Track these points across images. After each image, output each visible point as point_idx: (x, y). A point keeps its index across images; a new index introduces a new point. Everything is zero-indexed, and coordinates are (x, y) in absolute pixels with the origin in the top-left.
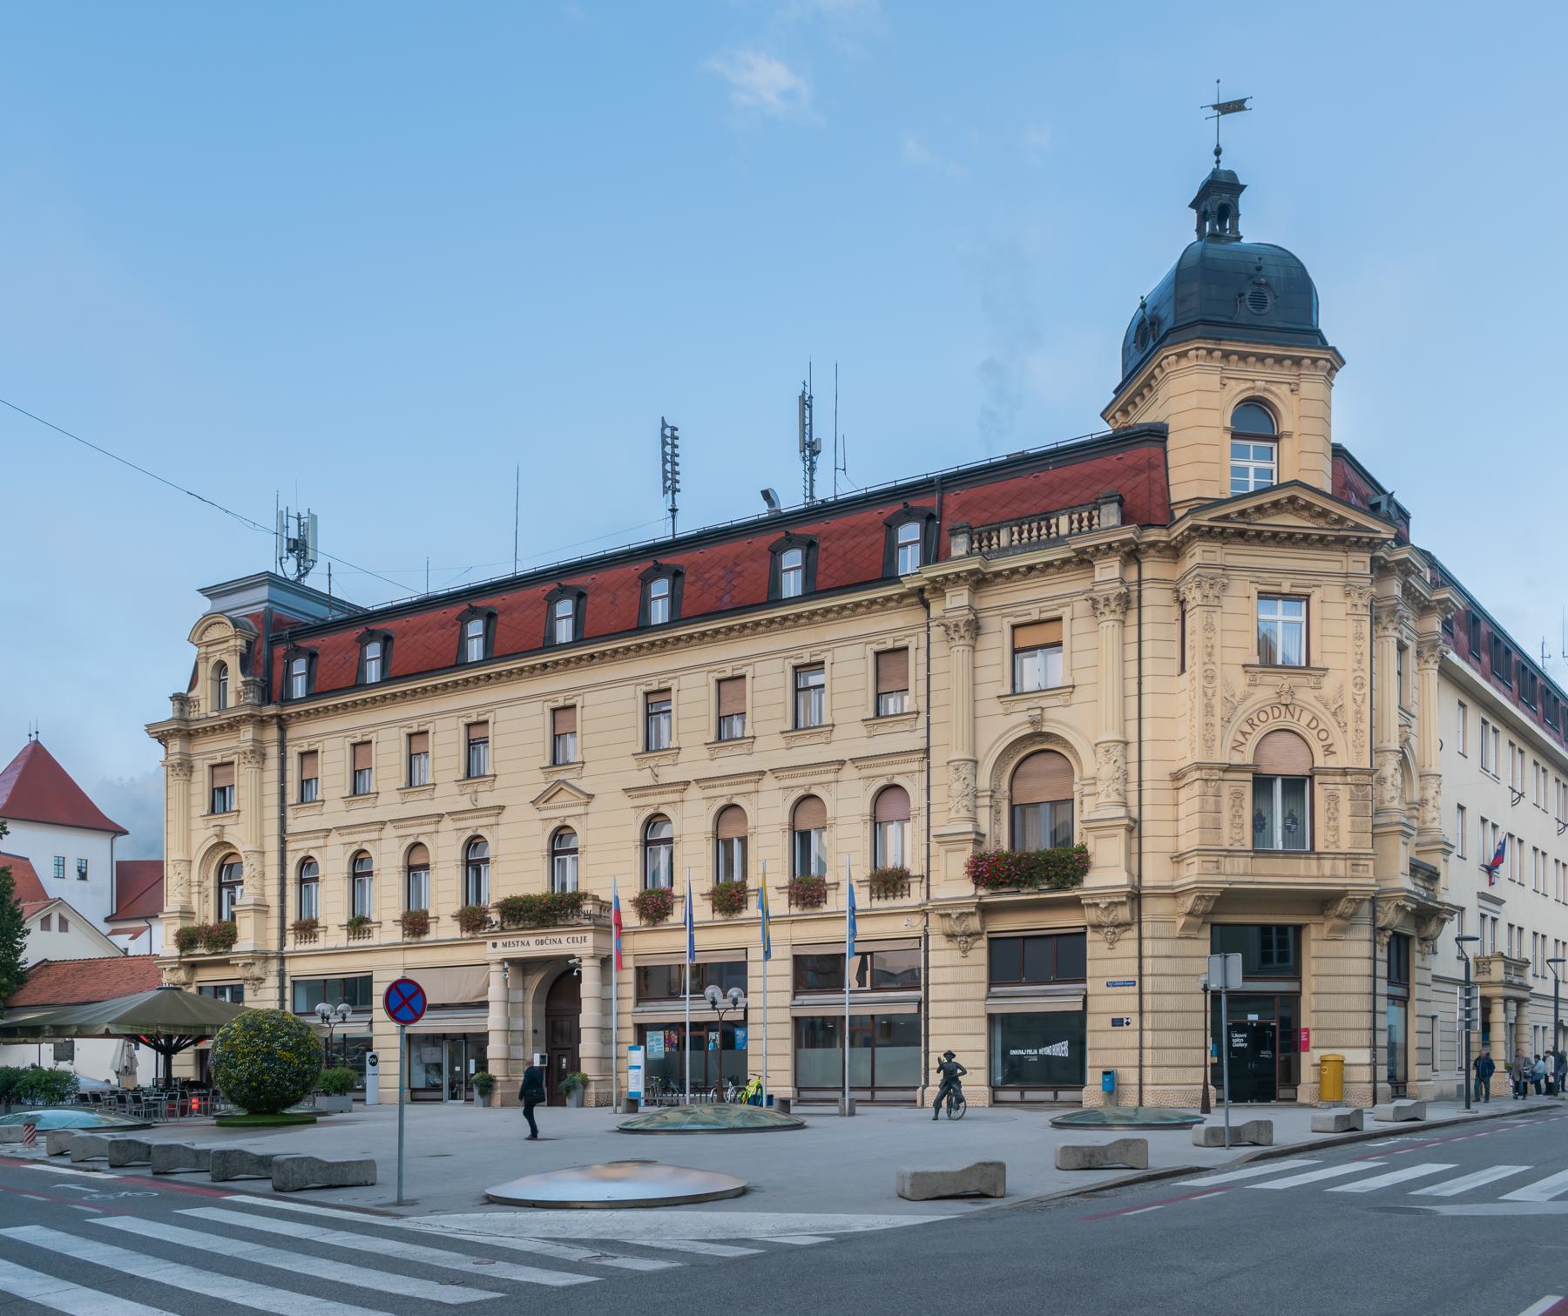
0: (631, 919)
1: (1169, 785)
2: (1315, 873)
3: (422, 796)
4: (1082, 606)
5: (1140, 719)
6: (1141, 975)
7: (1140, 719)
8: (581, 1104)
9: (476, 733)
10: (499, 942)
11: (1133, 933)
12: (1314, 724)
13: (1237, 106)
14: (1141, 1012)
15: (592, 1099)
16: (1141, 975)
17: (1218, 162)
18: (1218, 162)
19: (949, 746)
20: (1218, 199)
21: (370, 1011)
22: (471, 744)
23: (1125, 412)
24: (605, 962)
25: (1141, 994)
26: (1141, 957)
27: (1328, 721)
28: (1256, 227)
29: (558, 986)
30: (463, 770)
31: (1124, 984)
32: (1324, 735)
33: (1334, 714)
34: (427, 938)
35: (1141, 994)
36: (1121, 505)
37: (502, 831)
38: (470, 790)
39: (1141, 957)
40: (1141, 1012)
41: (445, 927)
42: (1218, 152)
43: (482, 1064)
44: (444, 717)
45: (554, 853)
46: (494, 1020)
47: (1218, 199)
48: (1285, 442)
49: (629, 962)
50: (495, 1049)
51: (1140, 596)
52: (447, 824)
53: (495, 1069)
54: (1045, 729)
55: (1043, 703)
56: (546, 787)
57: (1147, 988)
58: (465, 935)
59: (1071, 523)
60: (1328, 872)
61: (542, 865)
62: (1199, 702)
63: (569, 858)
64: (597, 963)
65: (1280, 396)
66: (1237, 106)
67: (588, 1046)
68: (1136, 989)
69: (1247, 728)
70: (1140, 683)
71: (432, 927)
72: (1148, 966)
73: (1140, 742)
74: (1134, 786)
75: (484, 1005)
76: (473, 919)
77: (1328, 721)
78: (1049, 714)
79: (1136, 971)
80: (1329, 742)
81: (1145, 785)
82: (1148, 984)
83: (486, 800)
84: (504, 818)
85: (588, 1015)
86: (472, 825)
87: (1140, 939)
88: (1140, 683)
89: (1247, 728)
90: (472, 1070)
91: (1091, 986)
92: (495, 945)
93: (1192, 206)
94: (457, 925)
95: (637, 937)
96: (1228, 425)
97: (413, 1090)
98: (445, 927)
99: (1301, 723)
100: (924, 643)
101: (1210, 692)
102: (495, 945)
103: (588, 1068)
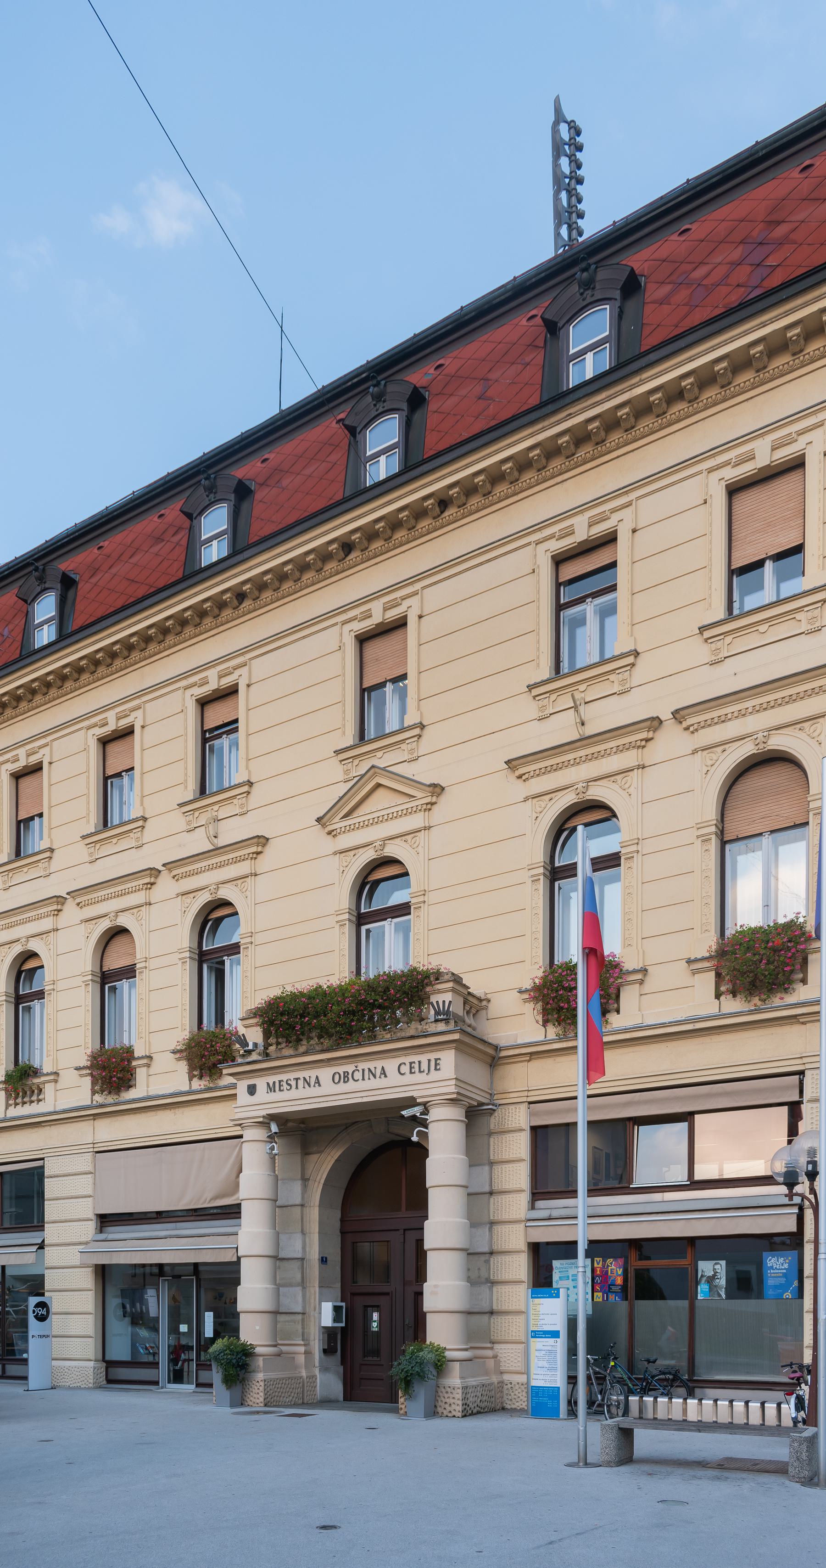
0: (517, 1023)
3: (124, 844)
8: (432, 1412)
9: (217, 715)
10: (261, 1083)
15: (454, 1402)
21: (41, 1227)
22: (208, 738)
24: (476, 1116)
29: (373, 1173)
30: (192, 785)
34: (132, 1094)
37: (262, 887)
38: (203, 819)
41: (163, 1073)
43: (228, 1323)
44: (158, 700)
45: (361, 919)
46: (251, 1236)
49: (520, 1118)
50: (252, 1293)
52: (166, 886)
53: (252, 1331)
56: (344, 788)
58: (197, 1084)
61: (340, 939)
63: (388, 926)
64: (458, 1113)
67: (443, 1289)
71: (141, 1074)
75: (233, 1212)
76: (209, 1054)
83: (233, 831)
84: (264, 863)
85: (443, 1223)
86: (209, 882)
90: (209, 1332)
92: (252, 1090)
94: (183, 1067)
95: (536, 1065)
97: (110, 1364)
98: (163, 1073)
102: (252, 1090)
103: (442, 1332)
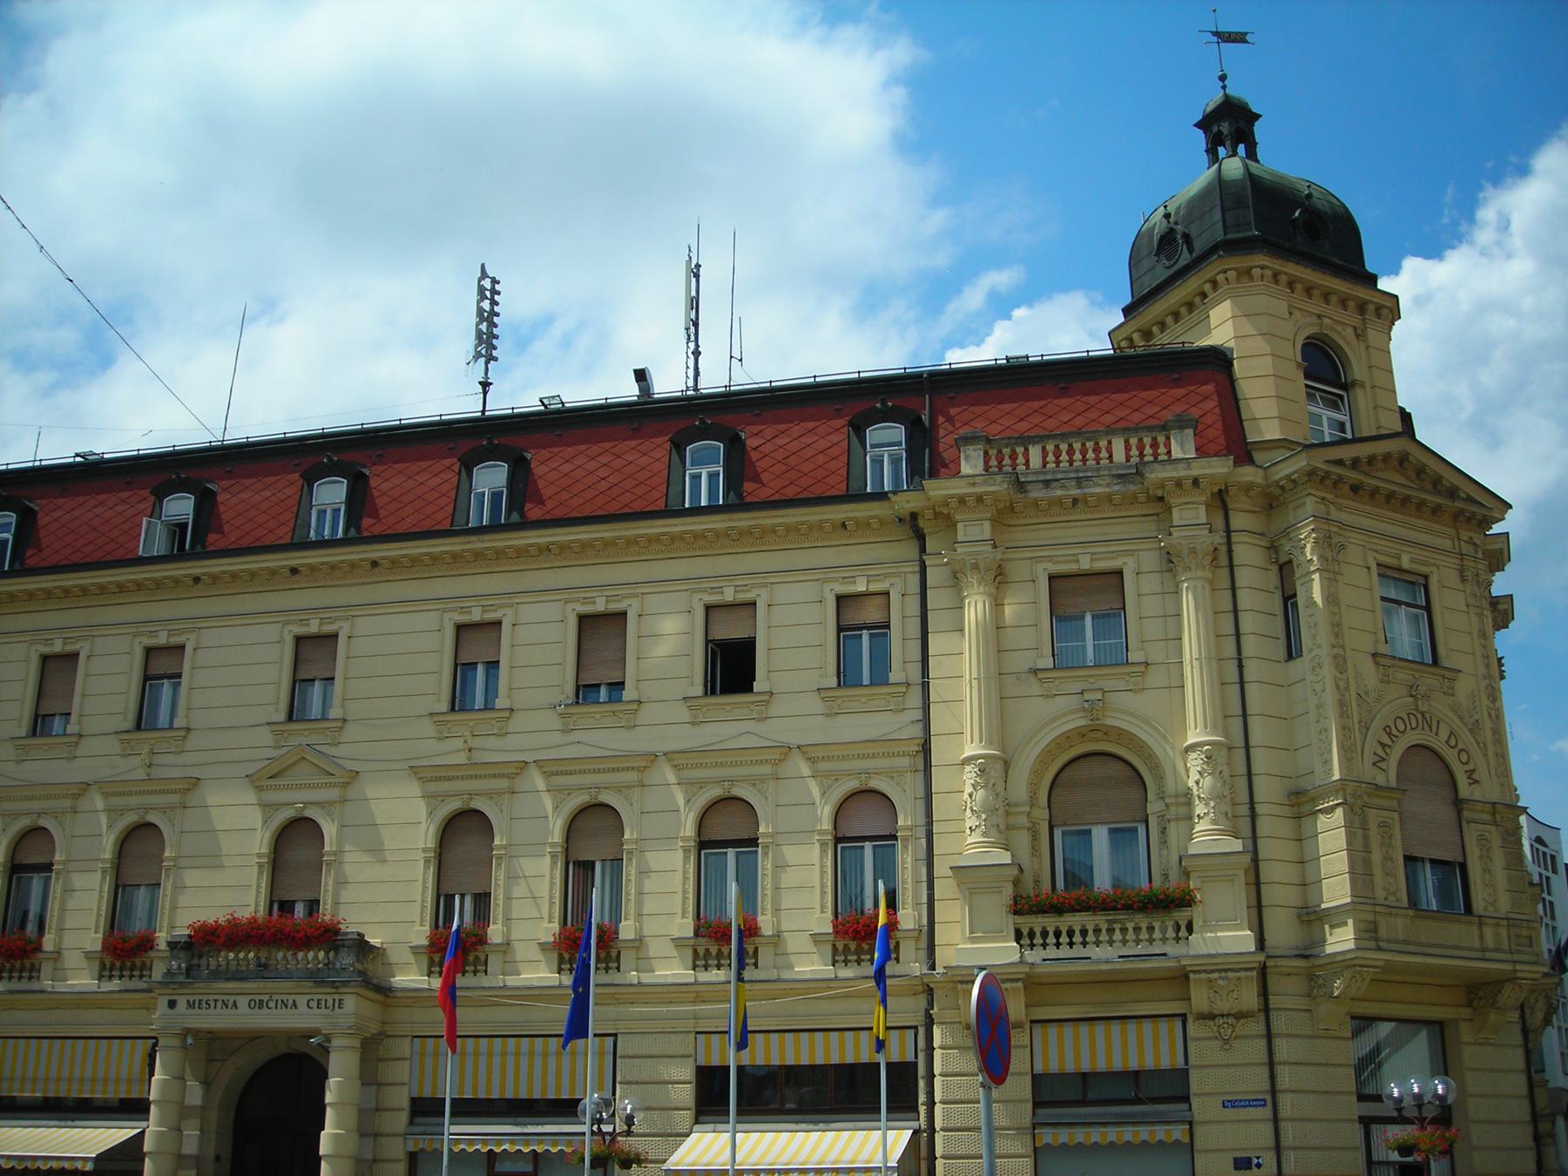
1: (1286, 811)
2: (1477, 944)
4: (1150, 560)
5: (1245, 716)
6: (1274, 1092)
7: (1245, 716)
11: (1257, 1027)
12: (1453, 742)
13: (1239, 38)
14: (1278, 1149)
16: (1274, 1092)
17: (1224, 87)
18: (1224, 87)
19: (963, 737)
20: (1230, 124)
23: (1147, 334)
25: (1276, 1120)
26: (1271, 1064)
27: (1467, 739)
28: (1284, 153)
31: (1249, 1104)
32: (1464, 758)
33: (1471, 731)
35: (1276, 1120)
36: (1195, 429)
39: (1271, 1064)
40: (1278, 1149)
42: (1223, 78)
47: (1230, 124)
48: (1359, 392)
51: (1230, 552)
54: (1109, 722)
55: (1108, 684)
57: (1286, 1109)
59: (1128, 448)
60: (1490, 943)
62: (1330, 697)
65: (1344, 338)
66: (1239, 38)
68: (1267, 1112)
69: (1387, 741)
70: (1240, 667)
72: (1285, 1077)
73: (1247, 747)
74: (1245, 810)
77: (1467, 739)
78: (1111, 697)
79: (1266, 1086)
80: (1471, 767)
81: (1260, 809)
82: (1287, 1105)
87: (1269, 1036)
88: (1240, 667)
89: (1387, 741)
91: (1203, 1107)
93: (1198, 125)
96: (1299, 359)
99: (1438, 743)
100: (914, 586)
101: (1342, 684)
